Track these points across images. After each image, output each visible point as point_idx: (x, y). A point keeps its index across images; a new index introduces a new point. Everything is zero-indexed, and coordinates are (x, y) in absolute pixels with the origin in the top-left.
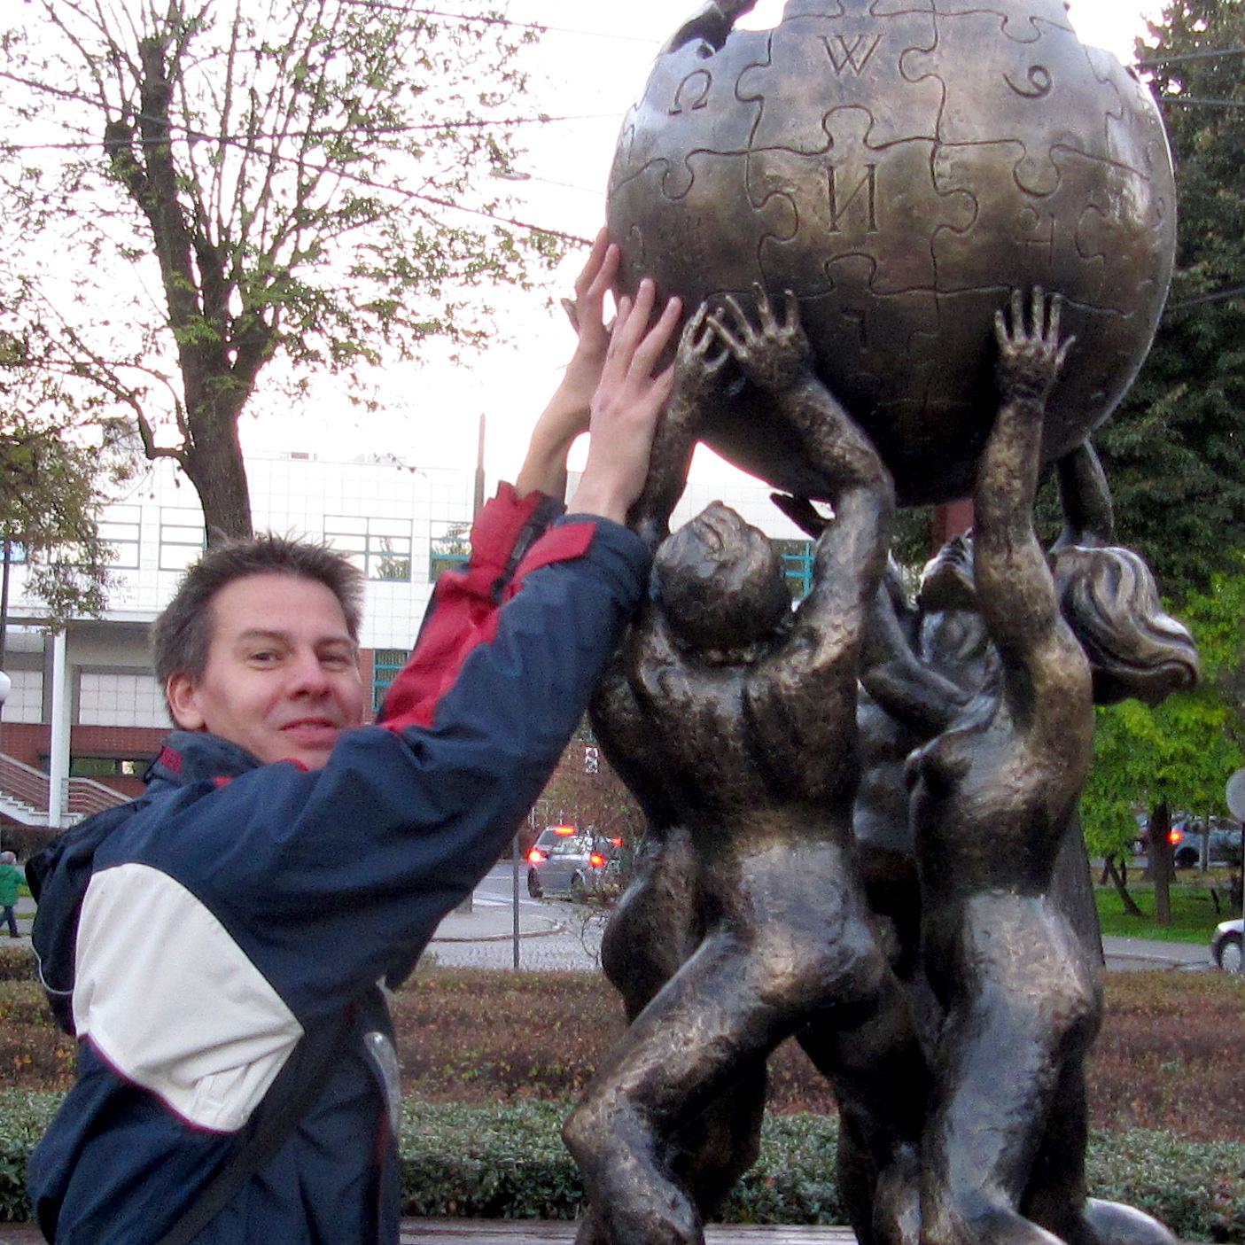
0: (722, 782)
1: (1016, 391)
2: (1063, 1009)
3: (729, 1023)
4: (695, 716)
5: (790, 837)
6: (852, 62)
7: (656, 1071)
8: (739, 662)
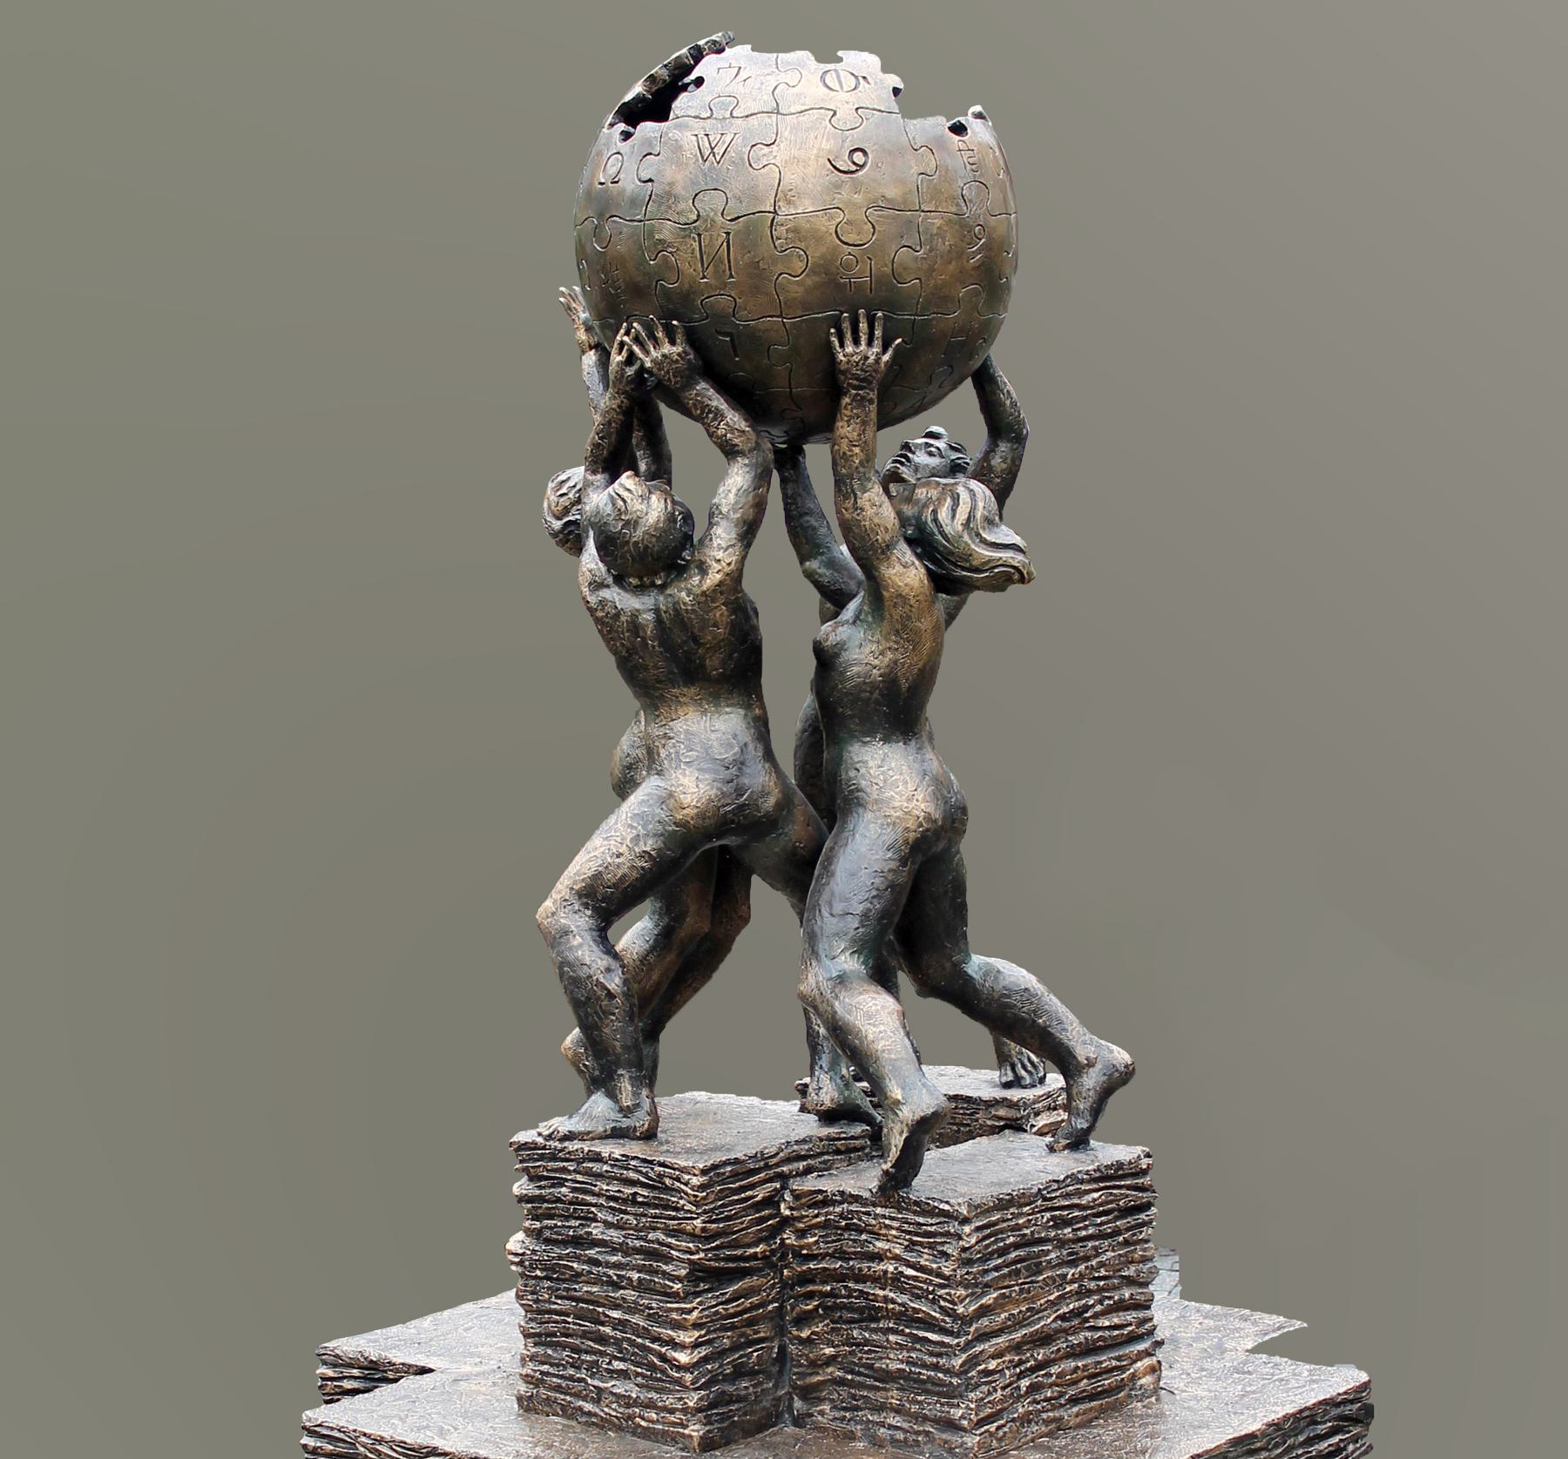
0: (646, 668)
1: (849, 384)
2: (911, 824)
3: (650, 842)
4: (623, 624)
5: (700, 705)
6: (714, 156)
7: (597, 876)
8: (653, 585)
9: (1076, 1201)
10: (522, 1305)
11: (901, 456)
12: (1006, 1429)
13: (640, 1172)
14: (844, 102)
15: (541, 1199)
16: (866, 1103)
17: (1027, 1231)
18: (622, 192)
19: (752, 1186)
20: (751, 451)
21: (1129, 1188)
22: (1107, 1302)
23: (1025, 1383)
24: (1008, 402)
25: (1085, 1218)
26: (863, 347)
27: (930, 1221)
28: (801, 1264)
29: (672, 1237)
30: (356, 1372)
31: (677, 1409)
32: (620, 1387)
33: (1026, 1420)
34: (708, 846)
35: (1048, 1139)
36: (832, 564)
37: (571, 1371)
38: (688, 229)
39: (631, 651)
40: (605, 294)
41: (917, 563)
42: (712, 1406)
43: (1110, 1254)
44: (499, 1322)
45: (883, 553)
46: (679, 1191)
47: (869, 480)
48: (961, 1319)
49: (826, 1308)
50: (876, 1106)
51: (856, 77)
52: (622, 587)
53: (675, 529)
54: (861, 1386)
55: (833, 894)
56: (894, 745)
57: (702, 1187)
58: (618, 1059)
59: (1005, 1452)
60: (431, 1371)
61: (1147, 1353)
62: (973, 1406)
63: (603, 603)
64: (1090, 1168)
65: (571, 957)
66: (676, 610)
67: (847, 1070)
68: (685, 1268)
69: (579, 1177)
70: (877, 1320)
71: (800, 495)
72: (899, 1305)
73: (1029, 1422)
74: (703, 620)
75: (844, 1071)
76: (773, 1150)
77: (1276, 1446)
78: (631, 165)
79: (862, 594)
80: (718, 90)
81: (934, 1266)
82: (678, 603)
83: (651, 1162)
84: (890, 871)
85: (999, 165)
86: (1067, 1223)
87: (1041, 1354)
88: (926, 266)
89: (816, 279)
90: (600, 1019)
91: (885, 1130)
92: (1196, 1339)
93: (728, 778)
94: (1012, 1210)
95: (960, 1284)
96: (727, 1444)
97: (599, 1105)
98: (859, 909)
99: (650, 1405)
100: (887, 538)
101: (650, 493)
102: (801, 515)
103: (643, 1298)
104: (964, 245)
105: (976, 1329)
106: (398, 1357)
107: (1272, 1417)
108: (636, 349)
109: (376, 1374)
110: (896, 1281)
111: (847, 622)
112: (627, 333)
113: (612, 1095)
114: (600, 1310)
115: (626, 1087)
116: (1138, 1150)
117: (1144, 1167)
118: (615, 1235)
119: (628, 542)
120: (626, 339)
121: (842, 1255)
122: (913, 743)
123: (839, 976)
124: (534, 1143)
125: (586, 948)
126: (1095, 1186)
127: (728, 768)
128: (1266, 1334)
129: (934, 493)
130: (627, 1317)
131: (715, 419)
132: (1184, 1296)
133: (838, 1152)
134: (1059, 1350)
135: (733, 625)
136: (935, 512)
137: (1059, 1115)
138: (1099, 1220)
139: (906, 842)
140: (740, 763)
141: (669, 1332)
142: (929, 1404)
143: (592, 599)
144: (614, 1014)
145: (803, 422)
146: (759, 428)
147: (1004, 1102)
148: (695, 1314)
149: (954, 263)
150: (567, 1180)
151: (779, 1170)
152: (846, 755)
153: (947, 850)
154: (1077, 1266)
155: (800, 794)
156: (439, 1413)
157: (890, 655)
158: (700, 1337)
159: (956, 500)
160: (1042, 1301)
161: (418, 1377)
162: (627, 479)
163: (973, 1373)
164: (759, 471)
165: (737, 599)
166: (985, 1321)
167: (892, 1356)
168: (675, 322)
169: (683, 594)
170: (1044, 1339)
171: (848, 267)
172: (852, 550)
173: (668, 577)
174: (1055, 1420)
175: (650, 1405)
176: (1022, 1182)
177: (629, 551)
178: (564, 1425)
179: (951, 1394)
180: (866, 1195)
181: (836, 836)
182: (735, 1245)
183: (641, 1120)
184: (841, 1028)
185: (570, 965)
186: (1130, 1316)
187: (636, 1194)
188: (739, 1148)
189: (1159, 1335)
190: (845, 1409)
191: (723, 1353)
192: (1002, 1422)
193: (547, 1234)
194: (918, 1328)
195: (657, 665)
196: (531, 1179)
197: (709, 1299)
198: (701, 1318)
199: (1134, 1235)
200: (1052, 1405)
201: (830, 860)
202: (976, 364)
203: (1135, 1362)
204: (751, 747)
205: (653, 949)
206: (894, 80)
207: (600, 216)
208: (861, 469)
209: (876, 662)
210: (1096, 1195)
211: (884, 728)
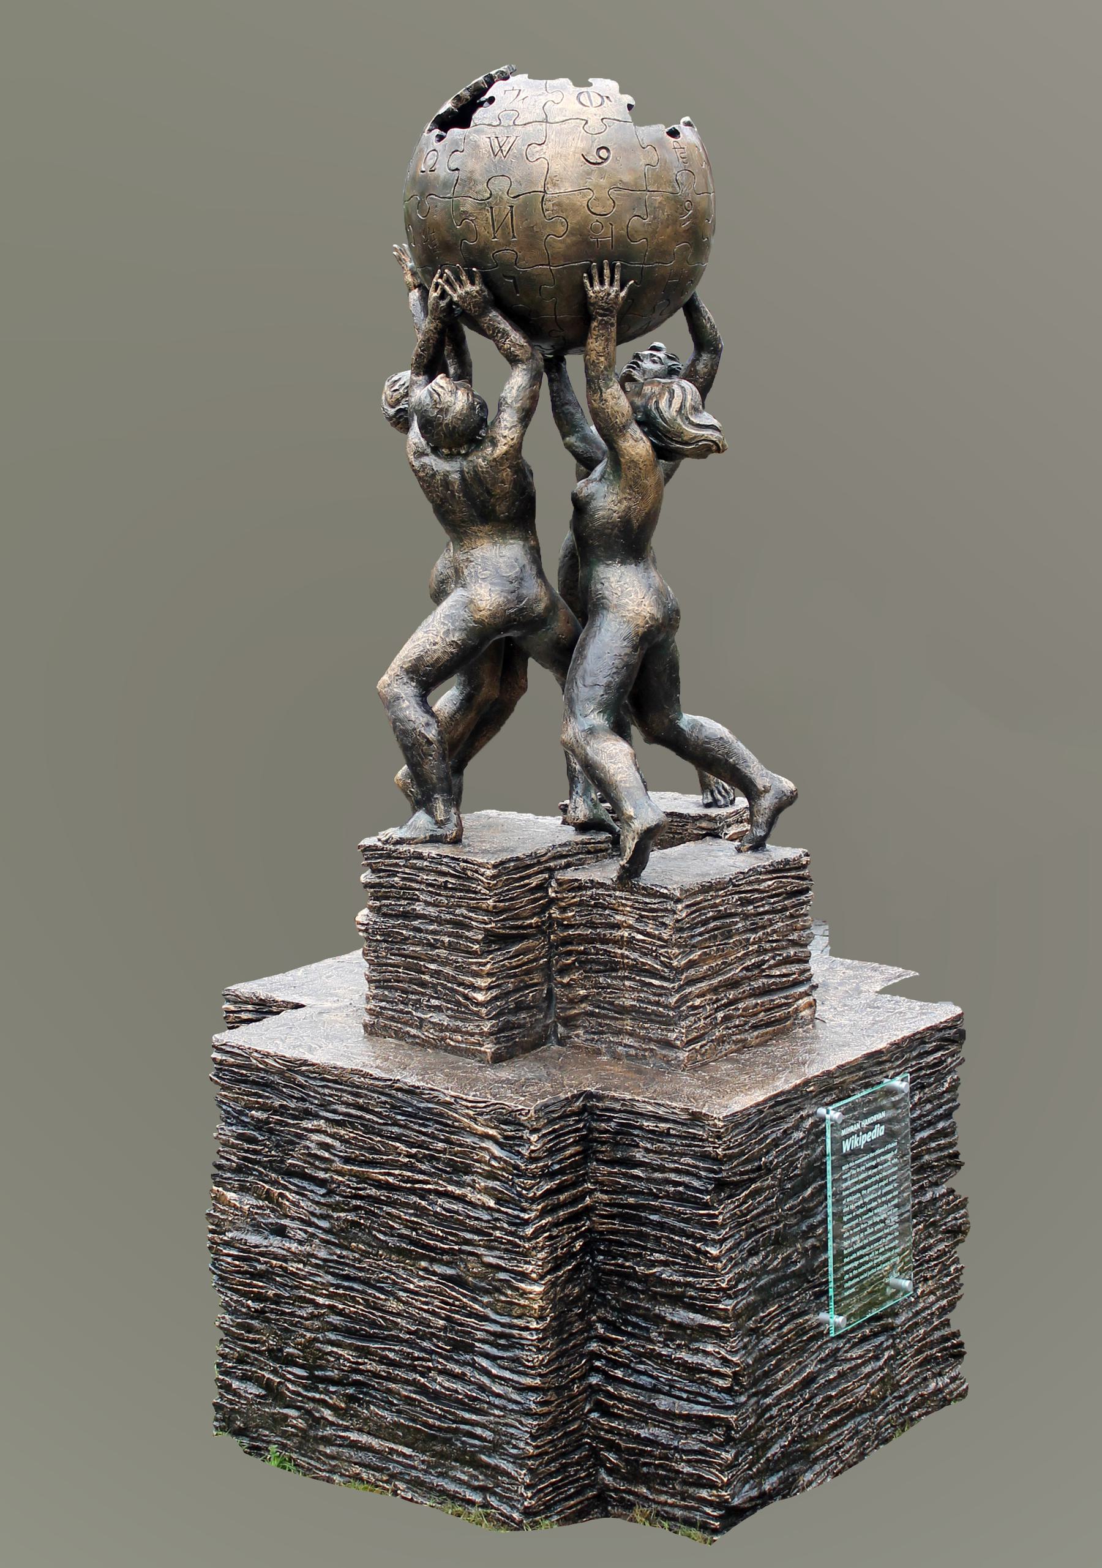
0: (454, 512)
1: (597, 313)
2: (640, 622)
3: (457, 634)
7: (420, 658)
8: (459, 454)
9: (756, 887)
10: (367, 960)
11: (633, 363)
12: (707, 1047)
13: (450, 866)
14: (593, 114)
15: (380, 885)
16: (608, 818)
17: (722, 908)
18: (437, 178)
19: (529, 877)
20: (527, 360)
21: (793, 877)
22: (778, 958)
23: (720, 1015)
24: (708, 325)
25: (762, 899)
26: (606, 287)
27: (654, 901)
28: (563, 931)
29: (472, 912)
30: (250, 1007)
31: (476, 1033)
32: (436, 1018)
33: (721, 1041)
34: (497, 638)
35: (737, 843)
36: (585, 439)
37: (401, 1007)
38: (483, 204)
39: (444, 500)
40: (425, 249)
41: (644, 438)
42: (500, 1031)
43: (780, 924)
44: (351, 972)
45: (620, 431)
46: (477, 880)
47: (611, 380)
48: (675, 970)
49: (580, 962)
50: (615, 820)
51: (602, 97)
52: (437, 456)
53: (474, 414)
54: (606, 1017)
55: (585, 671)
56: (628, 566)
57: (493, 877)
58: (434, 787)
59: (707, 1064)
60: (303, 1006)
61: (807, 994)
62: (684, 1031)
63: (424, 466)
64: (766, 863)
65: (401, 715)
66: (475, 471)
67: (595, 795)
68: (481, 934)
69: (407, 870)
70: (617, 971)
71: (562, 391)
72: (632, 960)
73: (723, 1042)
74: (494, 478)
75: (593, 796)
76: (543, 851)
77: (897, 1059)
78: (443, 159)
79: (606, 460)
80: (505, 106)
81: (657, 932)
82: (476, 466)
83: (457, 859)
84: (626, 654)
85: (702, 158)
86: (750, 902)
87: (731, 995)
88: (651, 230)
89: (574, 239)
90: (422, 759)
91: (622, 837)
92: (841, 984)
93: (512, 589)
94: (711, 893)
95: (674, 945)
96: (511, 1057)
97: (421, 819)
98: (604, 681)
99: (457, 1030)
100: (624, 421)
101: (457, 389)
102: (563, 405)
103: (452, 955)
104: (678, 214)
105: (686, 977)
106: (280, 997)
107: (894, 1039)
108: (447, 288)
109: (264, 1009)
110: (630, 943)
111: (595, 480)
112: (441, 277)
113: (430, 812)
114: (422, 963)
115: (440, 807)
116: (800, 851)
117: (804, 863)
118: (432, 911)
119: (441, 424)
120: (440, 281)
121: (592, 925)
122: (642, 565)
123: (590, 729)
124: (375, 846)
125: (412, 709)
126: (770, 876)
127: (512, 583)
128: (889, 980)
129: (656, 389)
130: (441, 968)
131: (502, 337)
132: (832, 953)
133: (589, 852)
134: (744, 992)
135: (515, 483)
136: (657, 402)
137: (744, 826)
138: (772, 900)
139: (637, 634)
140: (520, 579)
141: (471, 979)
142: (653, 1029)
143: (416, 464)
144: (431, 756)
145: (564, 339)
146: (534, 344)
147: (706, 817)
148: (489, 966)
149: (670, 227)
150: (398, 872)
151: (547, 865)
152: (594, 573)
153: (665, 640)
154: (757, 933)
155: (562, 599)
156: (309, 1036)
157: (625, 503)
158: (492, 982)
159: (672, 394)
160: (732, 957)
161: (294, 1011)
162: (440, 380)
163: (684, 1008)
164: (533, 374)
165: (518, 463)
166: (692, 972)
167: (627, 996)
168: (474, 269)
169: (480, 460)
170: (734, 984)
171: (596, 230)
172: (599, 429)
173: (470, 448)
174: (741, 1041)
175: (457, 1030)
176: (718, 874)
177: (442, 430)
178: (396, 1045)
179: (668, 1023)
180: (609, 882)
181: (588, 630)
182: (516, 918)
183: (450, 830)
184: (591, 765)
185: (400, 721)
186: (794, 968)
187: (447, 881)
188: (519, 850)
189: (815, 981)
190: (594, 1033)
191: (508, 994)
192: (704, 1042)
193: (385, 910)
194: (645, 976)
195: (462, 510)
196: (373, 871)
197: (499, 956)
198: (493, 969)
199: (797, 910)
200: (740, 1030)
201: (583, 647)
202: (686, 298)
203: (798, 1000)
204: (528, 568)
205: (456, 712)
206: (629, 99)
207: (422, 194)
208: (605, 373)
209: (616, 508)
210: (770, 883)
211: (622, 555)
